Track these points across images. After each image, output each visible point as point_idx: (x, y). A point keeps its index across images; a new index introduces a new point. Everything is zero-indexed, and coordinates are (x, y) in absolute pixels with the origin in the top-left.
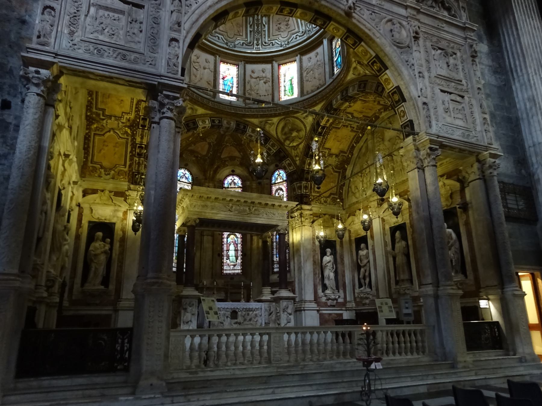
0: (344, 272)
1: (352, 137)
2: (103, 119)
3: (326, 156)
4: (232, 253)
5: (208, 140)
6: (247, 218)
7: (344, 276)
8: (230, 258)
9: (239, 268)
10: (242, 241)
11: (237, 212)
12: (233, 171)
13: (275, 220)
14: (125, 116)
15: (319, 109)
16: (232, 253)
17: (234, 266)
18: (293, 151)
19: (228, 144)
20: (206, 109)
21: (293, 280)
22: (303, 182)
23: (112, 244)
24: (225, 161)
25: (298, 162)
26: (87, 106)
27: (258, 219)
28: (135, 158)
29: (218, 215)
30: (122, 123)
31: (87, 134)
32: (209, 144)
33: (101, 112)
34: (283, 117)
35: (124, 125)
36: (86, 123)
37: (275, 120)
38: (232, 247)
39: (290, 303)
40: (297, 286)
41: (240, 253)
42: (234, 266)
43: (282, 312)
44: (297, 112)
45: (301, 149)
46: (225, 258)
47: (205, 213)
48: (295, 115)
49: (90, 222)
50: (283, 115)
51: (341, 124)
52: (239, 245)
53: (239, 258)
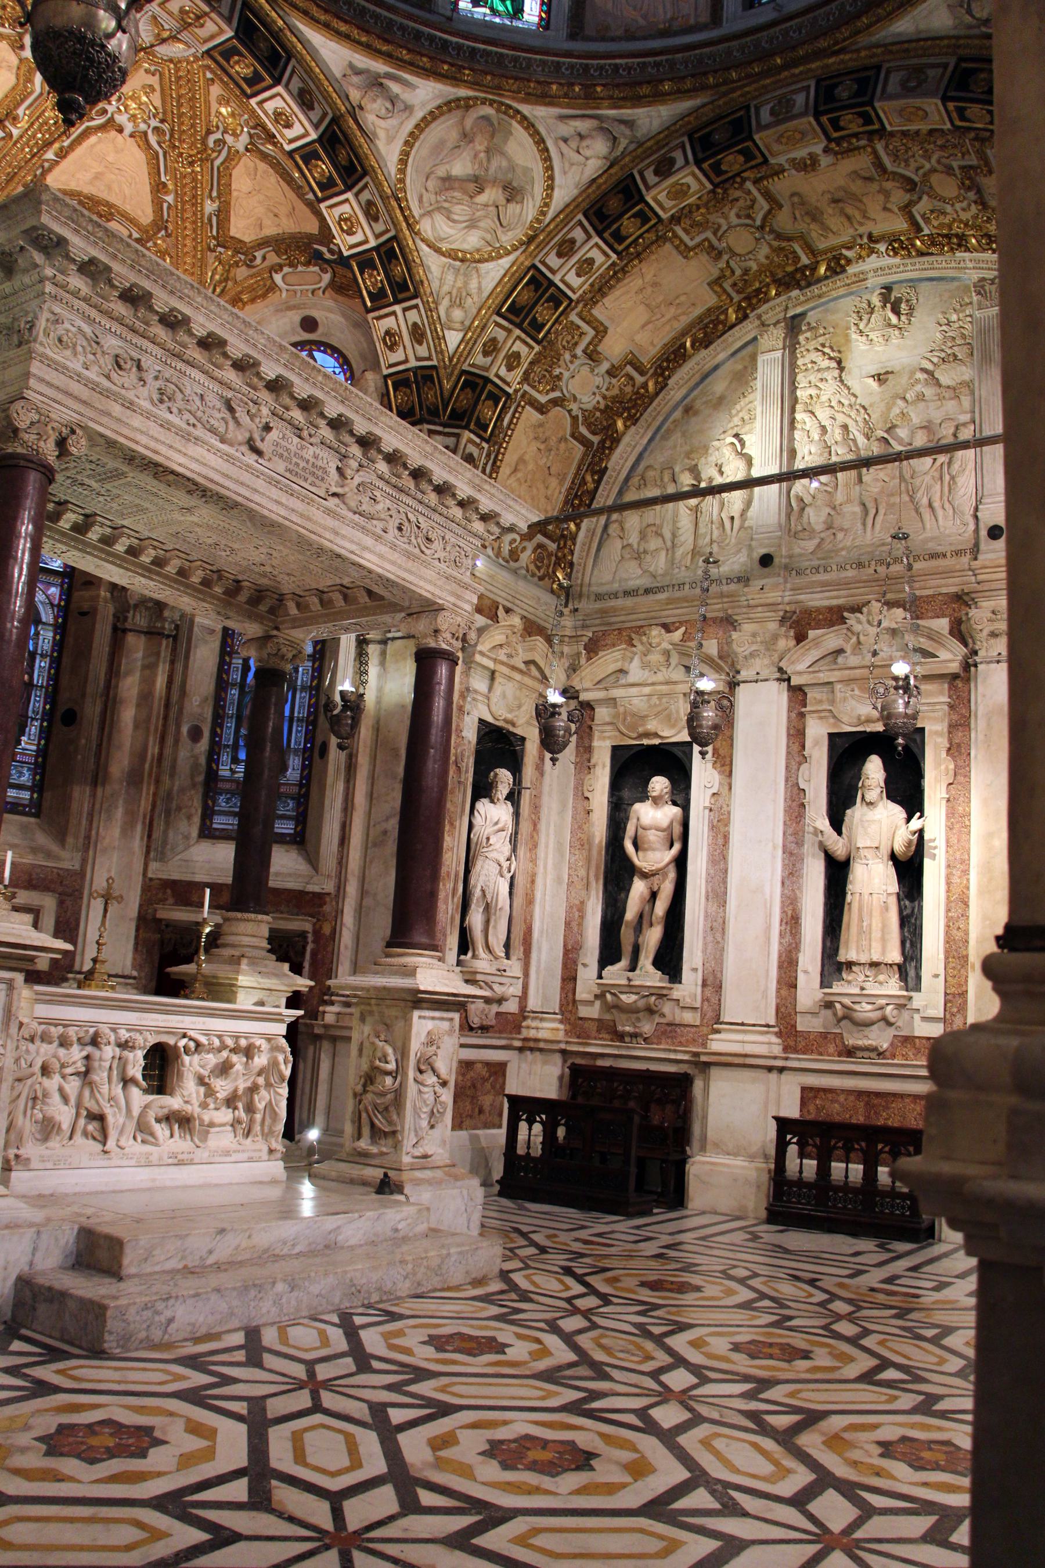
0: (533, 882)
1: (698, 311)
3: (579, 351)
6: (318, 515)
7: (530, 901)
9: (26, 778)
10: (59, 646)
11: (281, 466)
13: (430, 574)
15: (656, 125)
18: (450, 277)
19: (122, 119)
21: (329, 887)
22: (467, 435)
25: (453, 339)
27: (369, 541)
34: (463, 92)
37: (424, 93)
39: (446, 1025)
40: (348, 918)
43: (411, 1073)
44: (544, 98)
45: (489, 284)
47: (130, 406)
48: (525, 109)
50: (474, 85)
51: (709, 234)
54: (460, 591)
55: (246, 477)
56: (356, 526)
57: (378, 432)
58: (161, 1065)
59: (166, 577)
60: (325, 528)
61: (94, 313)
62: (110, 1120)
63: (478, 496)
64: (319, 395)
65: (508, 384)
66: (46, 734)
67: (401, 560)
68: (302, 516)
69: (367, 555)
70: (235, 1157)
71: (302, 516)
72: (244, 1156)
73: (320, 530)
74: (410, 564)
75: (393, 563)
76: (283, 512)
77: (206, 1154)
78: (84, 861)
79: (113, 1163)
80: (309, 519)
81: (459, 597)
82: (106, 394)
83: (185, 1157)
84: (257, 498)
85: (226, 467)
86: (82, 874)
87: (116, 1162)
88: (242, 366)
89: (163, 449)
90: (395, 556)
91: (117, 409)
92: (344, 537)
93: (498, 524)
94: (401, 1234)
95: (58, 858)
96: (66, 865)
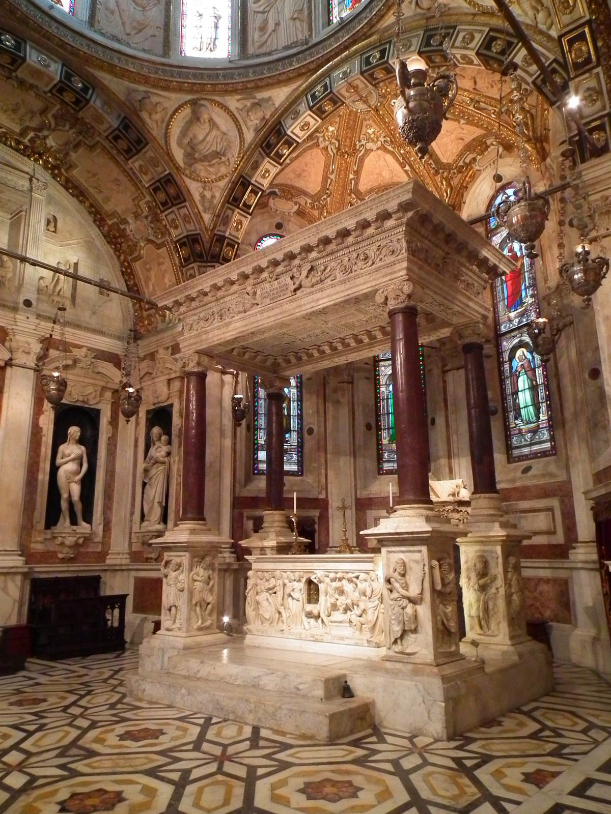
2: (125, 229)
4: (525, 398)
5: (370, 145)
8: (523, 411)
9: (546, 435)
11: (268, 301)
12: (498, 178)
13: (361, 280)
14: (141, 203)
16: (525, 398)
17: (535, 431)
20: (289, 80)
23: (169, 443)
24: (468, 165)
26: (94, 221)
27: (319, 295)
28: (184, 269)
29: (230, 328)
30: (146, 217)
31: (122, 265)
32: (383, 148)
33: (115, 220)
35: (149, 219)
36: (112, 251)
38: (523, 382)
39: (417, 556)
41: (542, 393)
42: (535, 431)
46: (512, 415)
49: (148, 412)
52: (539, 371)
53: (543, 408)
54: (389, 270)
55: (252, 319)
56: (321, 290)
57: (287, 250)
58: (313, 590)
59: (381, 341)
60: (294, 309)
61: (194, 312)
62: (284, 614)
63: (362, 217)
64: (255, 264)
65: (582, 18)
66: (549, 407)
67: (342, 287)
68: (281, 313)
69: (321, 302)
70: (346, 641)
71: (281, 313)
72: (353, 642)
73: (293, 312)
74: (348, 285)
75: (337, 293)
76: (272, 319)
77: (330, 638)
78: (569, 473)
79: (285, 636)
80: (285, 312)
81: (391, 274)
82: (199, 335)
83: (318, 637)
84: (261, 323)
85: (243, 323)
86: (569, 482)
87: (285, 636)
88: (232, 283)
89: (222, 336)
90: (338, 289)
91: (204, 337)
92: (305, 305)
93: (395, 213)
94: (302, 693)
95: (556, 476)
96: (560, 479)
